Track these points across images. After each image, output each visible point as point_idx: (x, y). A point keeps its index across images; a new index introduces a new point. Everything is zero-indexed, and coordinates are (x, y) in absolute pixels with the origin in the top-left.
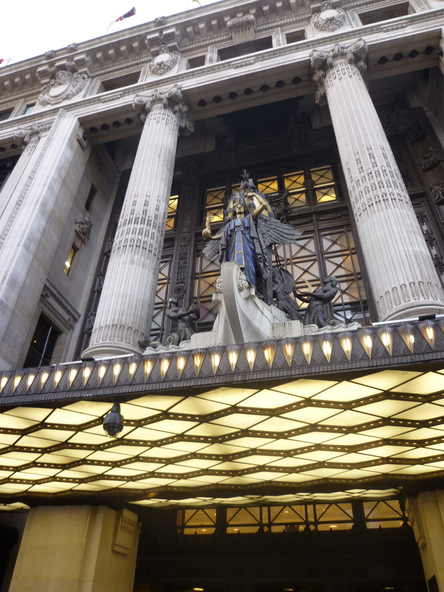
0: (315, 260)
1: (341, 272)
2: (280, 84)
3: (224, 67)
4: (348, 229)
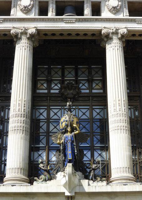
0: (89, 122)
1: (98, 117)
2: (85, 35)
3: (59, 20)
4: (105, 107)
